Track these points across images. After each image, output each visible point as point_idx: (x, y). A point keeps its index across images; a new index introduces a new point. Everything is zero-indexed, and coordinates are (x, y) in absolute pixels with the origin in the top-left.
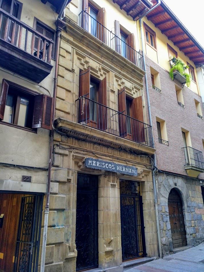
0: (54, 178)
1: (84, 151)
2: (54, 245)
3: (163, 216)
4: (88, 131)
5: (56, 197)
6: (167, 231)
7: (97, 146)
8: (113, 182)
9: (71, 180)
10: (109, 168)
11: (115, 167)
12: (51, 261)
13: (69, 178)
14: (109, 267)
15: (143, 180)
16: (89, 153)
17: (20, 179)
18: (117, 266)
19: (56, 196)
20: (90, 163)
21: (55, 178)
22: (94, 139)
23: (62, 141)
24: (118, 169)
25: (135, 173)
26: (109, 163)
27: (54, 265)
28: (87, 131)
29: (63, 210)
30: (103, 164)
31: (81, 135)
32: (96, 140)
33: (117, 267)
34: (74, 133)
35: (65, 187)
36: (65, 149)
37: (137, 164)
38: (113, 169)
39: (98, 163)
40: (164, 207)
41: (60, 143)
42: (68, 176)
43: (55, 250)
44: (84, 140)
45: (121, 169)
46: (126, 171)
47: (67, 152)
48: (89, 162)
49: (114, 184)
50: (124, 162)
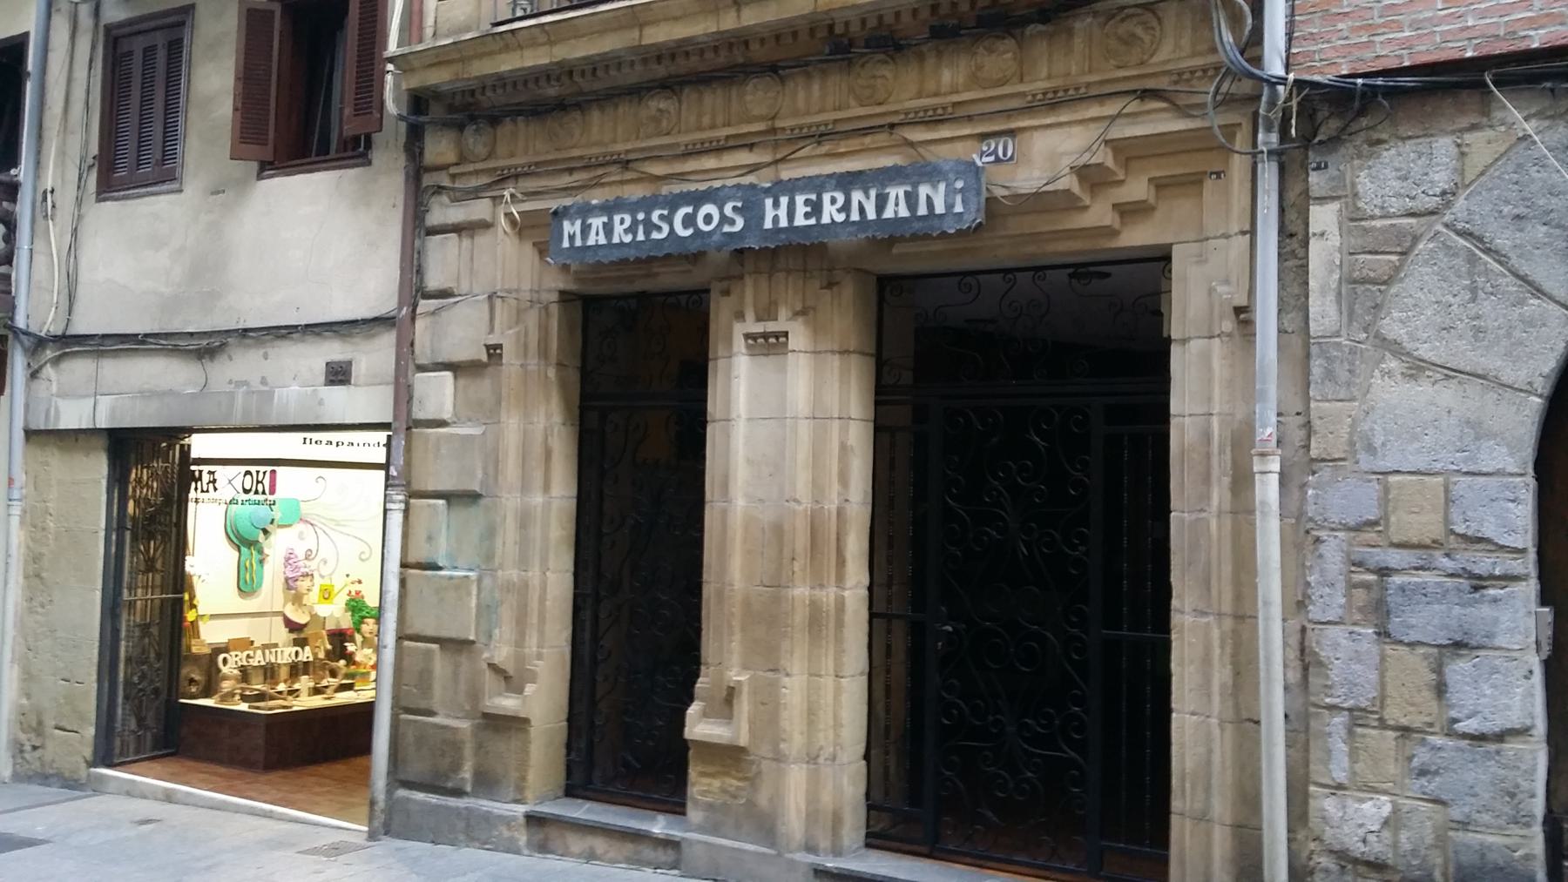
0: (429, 352)
1: (571, 171)
2: (435, 646)
3: (1397, 580)
4: (534, 44)
5: (439, 438)
6: (1438, 740)
7: (662, 106)
8: (766, 314)
9: (500, 346)
10: (698, 232)
11: (751, 210)
12: (423, 705)
13: (492, 340)
14: (715, 830)
15: (1138, 236)
16: (600, 172)
17: (322, 379)
18: (772, 845)
19: (431, 433)
20: (572, 238)
21: (433, 351)
22: (613, 73)
23: (462, 159)
24: (776, 219)
25: (949, 206)
26: (697, 199)
27: (436, 726)
28: (528, 53)
29: (472, 497)
30: (655, 217)
31: (548, 78)
32: (626, 70)
33: (764, 854)
34: (500, 91)
35: (482, 387)
36: (475, 194)
37: (1029, 110)
38: (727, 229)
39: (622, 222)
40: (1440, 479)
41: (453, 170)
42: (492, 330)
43: (440, 664)
44: (561, 106)
45: (801, 209)
46: (855, 217)
47: (479, 209)
48: (566, 225)
49: (771, 327)
50: (882, 138)
